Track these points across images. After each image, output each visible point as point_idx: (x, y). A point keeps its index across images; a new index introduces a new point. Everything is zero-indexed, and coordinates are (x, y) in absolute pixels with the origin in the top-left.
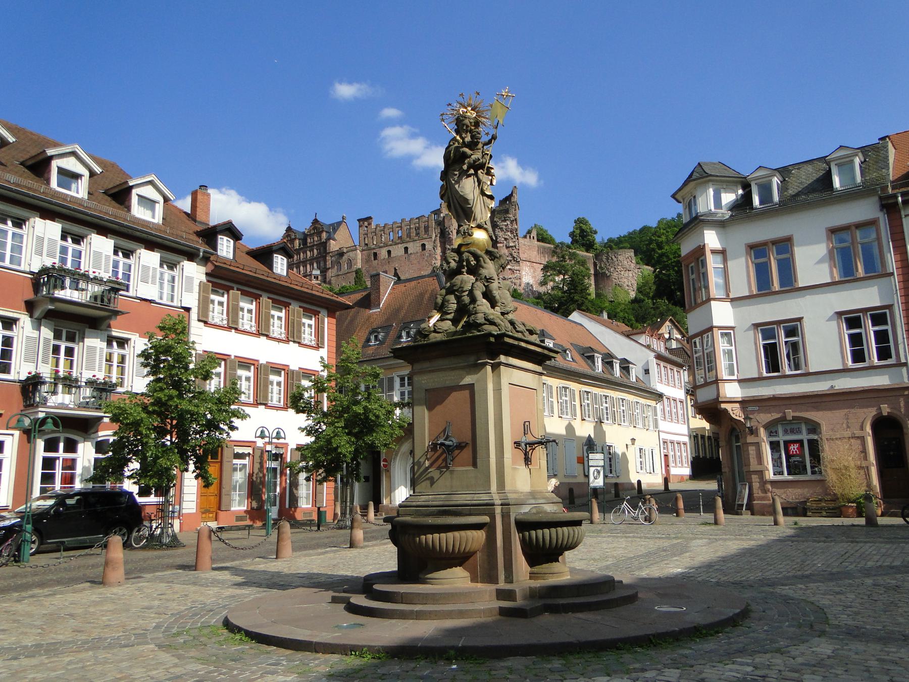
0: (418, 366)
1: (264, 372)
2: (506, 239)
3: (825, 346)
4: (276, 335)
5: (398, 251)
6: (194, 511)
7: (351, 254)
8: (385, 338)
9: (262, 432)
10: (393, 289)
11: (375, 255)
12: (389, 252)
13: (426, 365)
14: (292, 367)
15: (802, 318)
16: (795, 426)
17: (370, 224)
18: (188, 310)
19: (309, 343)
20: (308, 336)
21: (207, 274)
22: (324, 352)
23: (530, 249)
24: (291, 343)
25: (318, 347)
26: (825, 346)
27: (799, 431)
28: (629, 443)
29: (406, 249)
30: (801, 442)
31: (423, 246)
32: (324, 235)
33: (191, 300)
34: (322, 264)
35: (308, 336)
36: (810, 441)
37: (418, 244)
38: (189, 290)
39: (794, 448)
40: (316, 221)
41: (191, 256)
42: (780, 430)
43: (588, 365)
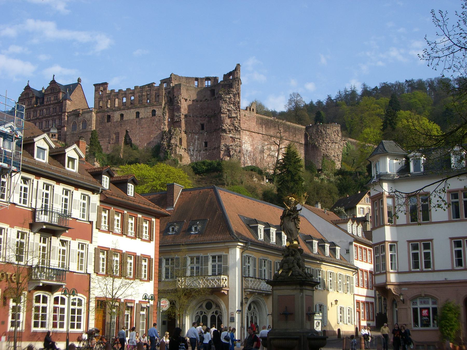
0: (275, 288)
1: (124, 256)
2: (228, 110)
3: (443, 256)
5: (130, 115)
7: (87, 116)
8: (179, 229)
9: (146, 296)
10: (181, 194)
11: (109, 117)
12: (122, 115)
13: (278, 287)
14: (138, 254)
15: (433, 239)
16: (426, 300)
17: (105, 89)
18: (91, 223)
20: (145, 235)
21: (101, 201)
22: (153, 243)
23: (249, 120)
24: (137, 239)
26: (443, 256)
27: (428, 303)
28: (334, 303)
29: (138, 114)
30: (428, 309)
31: (154, 111)
32: (61, 96)
33: (93, 217)
34: (57, 122)
35: (145, 235)
36: (433, 308)
37: (149, 110)
39: (425, 312)
41: (94, 191)
42: (418, 303)
43: (308, 248)
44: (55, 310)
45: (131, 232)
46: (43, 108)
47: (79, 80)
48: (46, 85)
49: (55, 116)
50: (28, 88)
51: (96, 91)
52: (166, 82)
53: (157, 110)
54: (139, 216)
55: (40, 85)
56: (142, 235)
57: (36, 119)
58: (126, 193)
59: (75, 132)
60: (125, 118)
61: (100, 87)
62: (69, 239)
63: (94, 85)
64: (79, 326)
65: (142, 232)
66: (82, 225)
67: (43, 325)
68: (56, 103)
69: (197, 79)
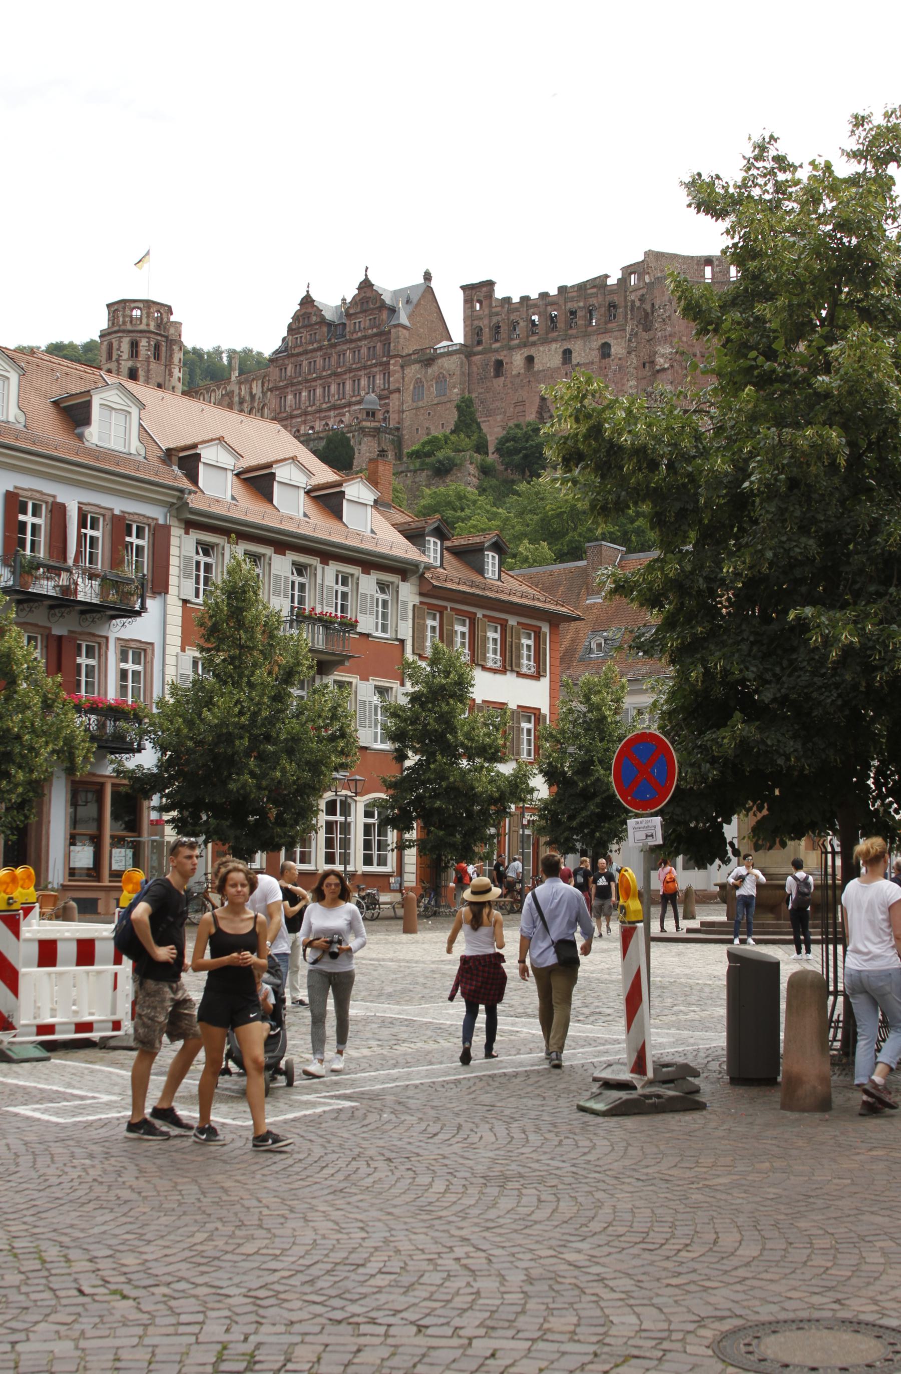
4: (490, 664)
6: (414, 884)
11: (499, 364)
12: (530, 360)
18: (402, 641)
19: (528, 672)
20: (527, 664)
22: (545, 682)
25: (537, 676)
29: (567, 353)
33: (406, 631)
34: (379, 381)
35: (527, 664)
37: (596, 343)
38: (405, 619)
40: (366, 285)
44: (330, 826)
45: (493, 658)
46: (345, 347)
47: (428, 277)
48: (350, 293)
49: (375, 365)
50: (307, 301)
51: (466, 301)
52: (634, 273)
53: (612, 341)
54: (512, 621)
55: (334, 295)
56: (519, 665)
57: (330, 376)
58: (483, 575)
59: (420, 404)
60: (537, 366)
61: (478, 293)
62: (354, 679)
63: (463, 288)
64: (382, 862)
65: (519, 657)
66: (381, 645)
67: (304, 859)
68: (375, 335)
69: (708, 261)
